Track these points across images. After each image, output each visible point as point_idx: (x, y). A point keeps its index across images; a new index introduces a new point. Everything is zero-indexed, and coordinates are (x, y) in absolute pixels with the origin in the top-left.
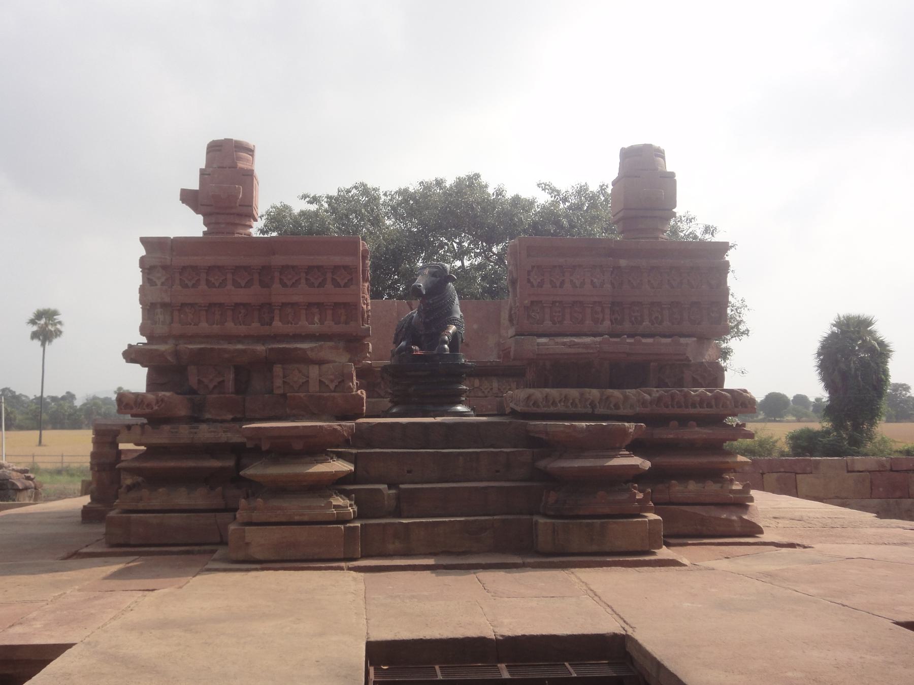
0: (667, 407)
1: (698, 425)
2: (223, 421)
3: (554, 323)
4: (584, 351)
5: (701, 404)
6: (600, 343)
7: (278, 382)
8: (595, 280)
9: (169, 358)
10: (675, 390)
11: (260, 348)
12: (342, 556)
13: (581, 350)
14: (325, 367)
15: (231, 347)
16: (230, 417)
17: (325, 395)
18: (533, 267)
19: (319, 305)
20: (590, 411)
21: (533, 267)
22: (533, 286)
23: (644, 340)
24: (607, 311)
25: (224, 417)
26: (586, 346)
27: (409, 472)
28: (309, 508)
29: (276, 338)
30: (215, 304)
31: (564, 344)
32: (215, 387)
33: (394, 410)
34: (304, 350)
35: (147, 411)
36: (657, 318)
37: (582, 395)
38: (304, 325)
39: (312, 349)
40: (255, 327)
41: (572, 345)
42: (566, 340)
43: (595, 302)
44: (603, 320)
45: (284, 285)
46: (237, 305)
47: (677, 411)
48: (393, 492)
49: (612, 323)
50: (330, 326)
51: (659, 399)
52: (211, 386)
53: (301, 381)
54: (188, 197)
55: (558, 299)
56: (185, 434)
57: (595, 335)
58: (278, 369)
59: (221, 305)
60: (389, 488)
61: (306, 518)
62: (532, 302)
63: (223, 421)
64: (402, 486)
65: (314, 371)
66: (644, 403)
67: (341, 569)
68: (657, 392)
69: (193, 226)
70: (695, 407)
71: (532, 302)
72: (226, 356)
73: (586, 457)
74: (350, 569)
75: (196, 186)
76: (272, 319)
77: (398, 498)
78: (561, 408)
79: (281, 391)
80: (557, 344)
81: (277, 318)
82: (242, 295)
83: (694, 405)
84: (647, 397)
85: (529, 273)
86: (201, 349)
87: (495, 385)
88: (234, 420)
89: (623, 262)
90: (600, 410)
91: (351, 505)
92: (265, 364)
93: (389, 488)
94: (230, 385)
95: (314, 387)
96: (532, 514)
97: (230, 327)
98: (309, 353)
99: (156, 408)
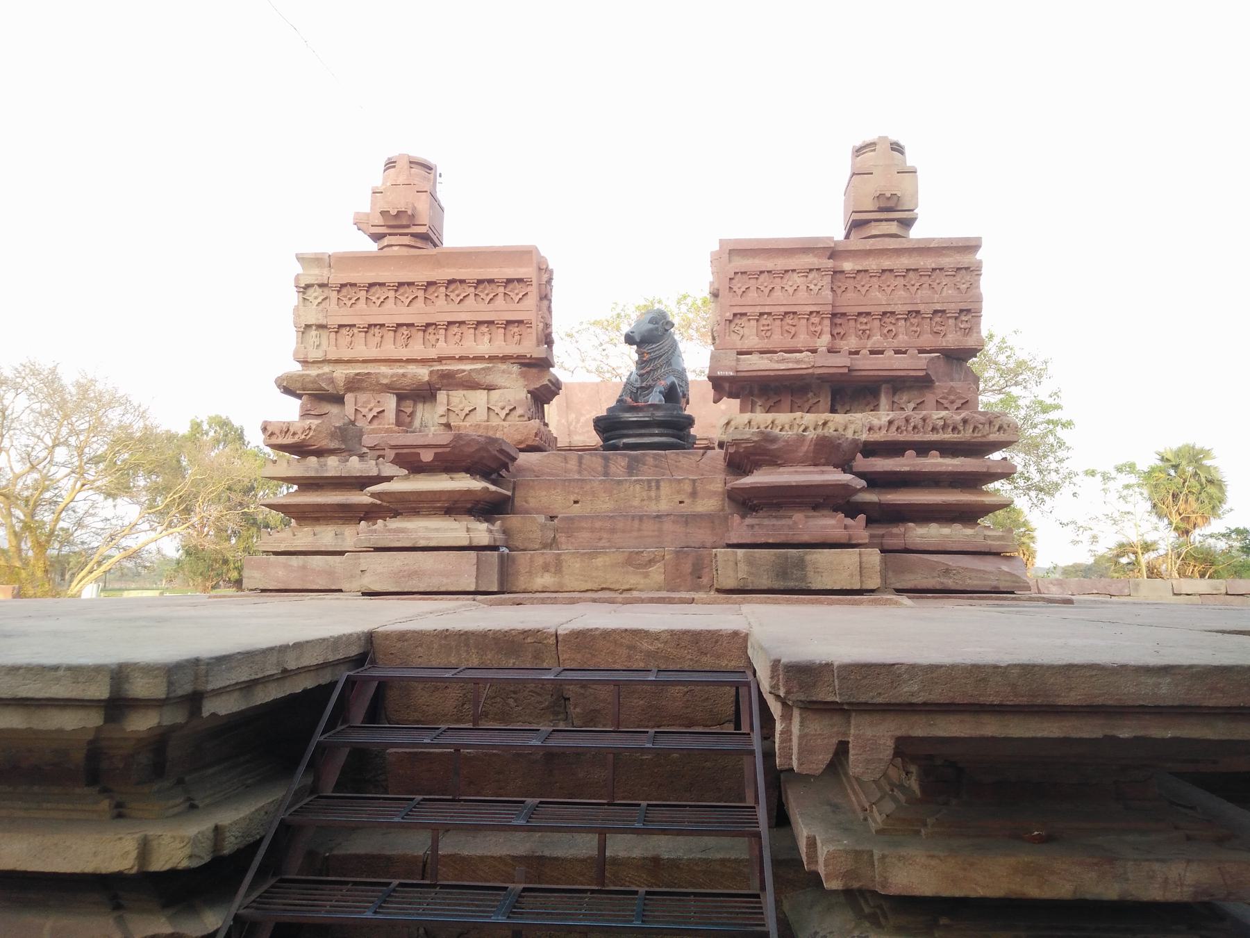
4: (796, 366)
5: (944, 427)
8: (812, 287)
12: (472, 588)
13: (791, 366)
18: (736, 273)
24: (827, 322)
26: (798, 362)
27: (576, 502)
43: (811, 313)
47: (917, 437)
51: (890, 422)
52: (370, 416)
53: (467, 410)
55: (767, 310)
56: (332, 466)
58: (442, 396)
61: (432, 544)
62: (735, 315)
65: (479, 398)
71: (735, 315)
72: (385, 381)
82: (403, 314)
83: (934, 429)
89: (848, 266)
94: (391, 415)
97: (390, 348)
98: (473, 374)
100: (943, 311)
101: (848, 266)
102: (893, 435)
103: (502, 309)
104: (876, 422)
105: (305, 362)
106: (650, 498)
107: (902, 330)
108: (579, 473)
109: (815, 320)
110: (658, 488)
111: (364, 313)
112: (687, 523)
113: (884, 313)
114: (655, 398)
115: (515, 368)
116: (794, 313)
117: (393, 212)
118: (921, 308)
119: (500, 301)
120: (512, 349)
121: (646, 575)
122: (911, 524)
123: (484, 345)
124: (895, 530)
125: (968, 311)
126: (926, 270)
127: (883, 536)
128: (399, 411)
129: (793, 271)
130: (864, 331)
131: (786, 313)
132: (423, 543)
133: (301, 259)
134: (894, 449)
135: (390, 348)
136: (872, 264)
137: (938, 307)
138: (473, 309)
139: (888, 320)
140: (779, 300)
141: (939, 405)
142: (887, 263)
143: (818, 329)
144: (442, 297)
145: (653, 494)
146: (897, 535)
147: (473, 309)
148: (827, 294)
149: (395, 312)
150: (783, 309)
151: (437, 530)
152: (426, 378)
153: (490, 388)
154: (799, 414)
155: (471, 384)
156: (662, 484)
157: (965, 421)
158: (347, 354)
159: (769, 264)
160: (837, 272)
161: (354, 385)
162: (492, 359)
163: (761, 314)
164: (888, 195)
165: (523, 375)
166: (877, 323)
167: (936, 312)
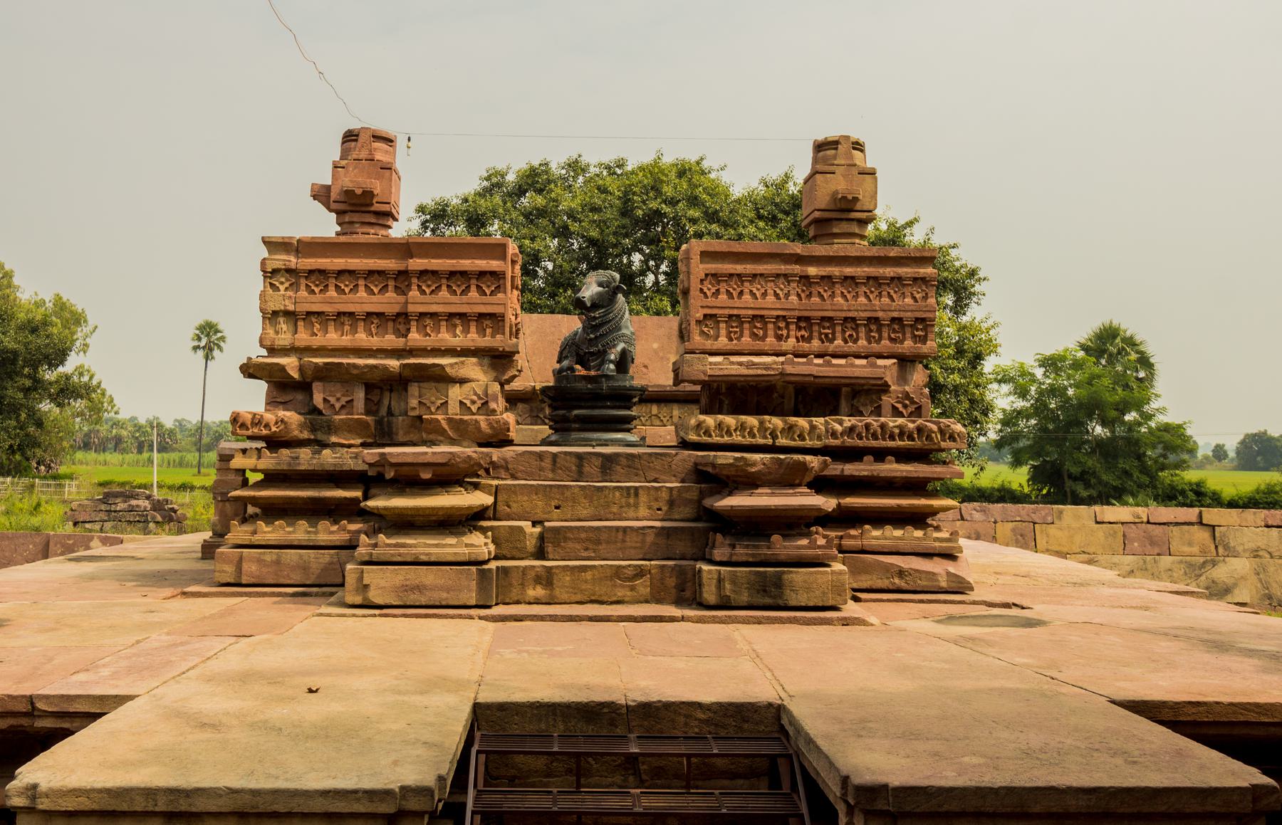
0: (861, 439)
1: (898, 461)
2: (350, 446)
3: (731, 340)
6: (783, 363)
7: (414, 402)
9: (292, 373)
10: (869, 420)
11: (394, 364)
12: (473, 602)
13: (759, 372)
15: (361, 362)
16: (359, 441)
17: (466, 418)
19: (462, 316)
20: (770, 441)
21: (707, 275)
22: (706, 297)
23: (835, 361)
25: (352, 442)
27: (557, 508)
28: (437, 546)
29: (412, 352)
30: (344, 313)
31: (740, 364)
32: (343, 407)
34: (442, 367)
35: (265, 432)
36: (851, 336)
37: (762, 423)
38: (445, 337)
39: (451, 365)
40: (390, 340)
41: (751, 365)
42: (744, 359)
43: (778, 317)
44: (788, 337)
45: (423, 293)
46: (369, 314)
47: (874, 443)
48: (538, 529)
49: (798, 341)
50: (473, 338)
51: (852, 429)
54: (321, 195)
55: (735, 312)
56: (305, 458)
57: (777, 355)
58: (414, 389)
59: (351, 314)
60: (534, 526)
62: (705, 316)
63: (350, 446)
64: (547, 524)
66: (834, 434)
67: (471, 618)
68: (848, 421)
69: (325, 225)
70: (894, 440)
71: (705, 316)
72: (355, 372)
73: (761, 495)
74: (480, 618)
75: (328, 181)
76: (408, 330)
77: (541, 538)
78: (737, 438)
79: (416, 413)
80: (733, 363)
81: (413, 329)
84: (838, 428)
85: (702, 281)
86: (326, 364)
87: (676, 412)
88: (364, 445)
89: (812, 271)
90: (782, 441)
91: (486, 544)
92: (399, 383)
93: (534, 526)
95: (454, 408)
96: (696, 560)
97: (362, 338)
98: (448, 370)
99: (274, 429)
100: (900, 320)
101: (812, 271)
103: (473, 301)
105: (272, 351)
106: (628, 505)
107: (862, 335)
108: (553, 471)
109: (782, 325)
110: (637, 495)
111: (330, 299)
112: (668, 536)
113: (846, 319)
115: (486, 361)
116: (762, 316)
117: (359, 192)
118: (880, 314)
119: (473, 294)
120: (487, 341)
121: (632, 589)
122: (867, 527)
123: (459, 339)
125: (923, 320)
126: (886, 278)
127: (841, 538)
128: (367, 400)
129: (761, 275)
130: (826, 335)
131: (754, 316)
132: (424, 558)
133: (267, 243)
134: (853, 454)
135: (362, 338)
136: (835, 271)
137: (895, 315)
138: (444, 301)
139: (849, 325)
140: (747, 303)
141: (897, 413)
142: (849, 271)
143: (785, 332)
144: (414, 287)
145: (632, 501)
146: (854, 537)
147: (444, 301)
149: (363, 300)
150: (750, 312)
151: (437, 546)
152: (397, 370)
153: (462, 381)
154: (767, 417)
156: (641, 492)
158: (317, 341)
159: (739, 268)
160: (805, 279)
163: (730, 316)
164: (850, 197)
165: (493, 366)
166: (839, 328)
167: (893, 320)
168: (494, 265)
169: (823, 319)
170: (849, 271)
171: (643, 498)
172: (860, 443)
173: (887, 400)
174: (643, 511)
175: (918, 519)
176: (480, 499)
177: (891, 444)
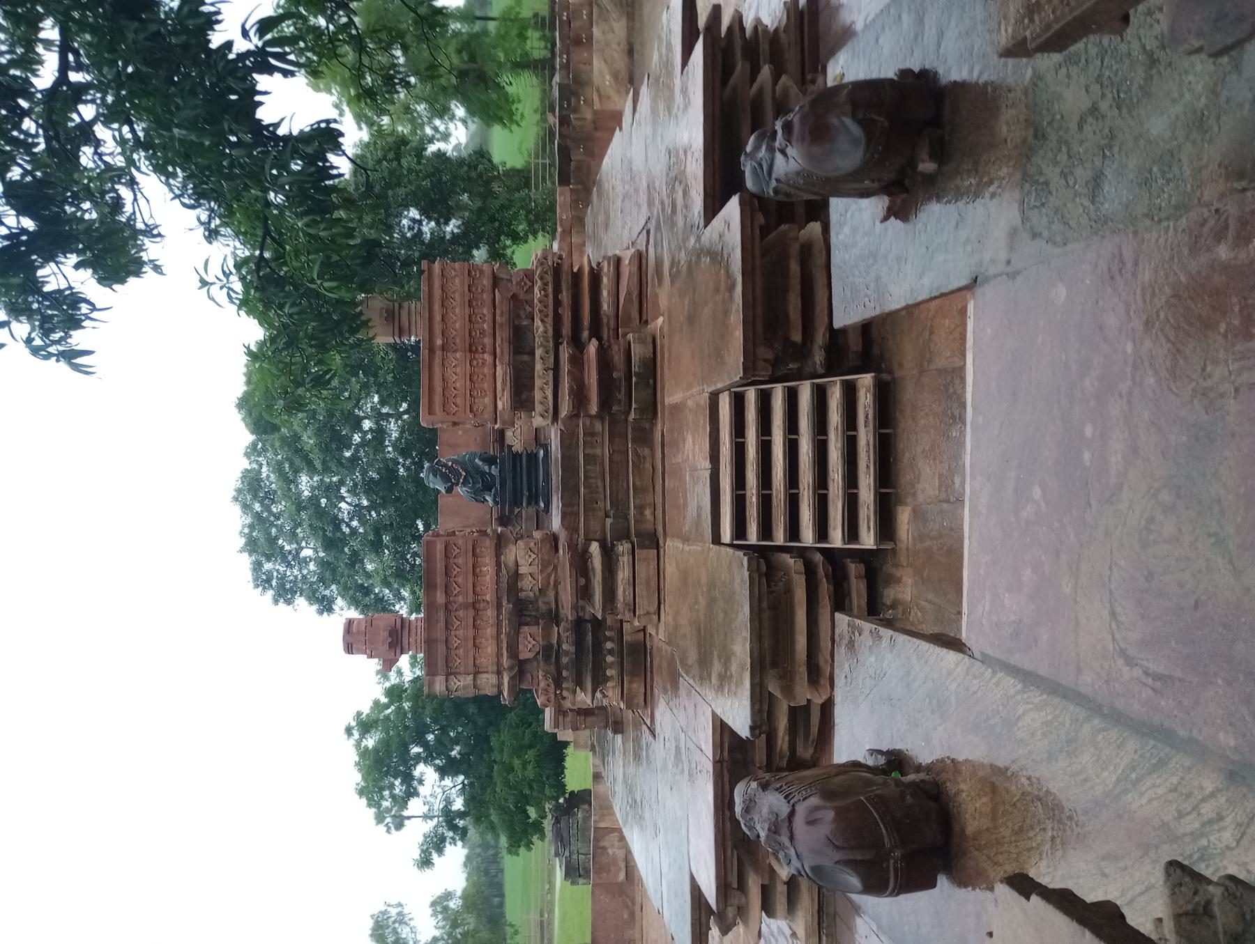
5: (544, 289)
14: (521, 562)
20: (551, 373)
33: (542, 505)
51: (542, 321)
83: (546, 296)
89: (439, 342)
101: (439, 342)
102: (550, 320)
104: (541, 329)
109: (475, 363)
114: (494, 470)
118: (467, 300)
124: (605, 321)
136: (438, 328)
142: (438, 318)
148: (458, 355)
150: (468, 382)
155: (516, 576)
157: (541, 279)
161: (513, 652)
162: (498, 564)
168: (440, 547)
169: (470, 335)
170: (438, 318)
171: (588, 451)
172: (551, 315)
173: (522, 296)
174: (598, 451)
175: (595, 277)
176: (595, 548)
177: (551, 296)
